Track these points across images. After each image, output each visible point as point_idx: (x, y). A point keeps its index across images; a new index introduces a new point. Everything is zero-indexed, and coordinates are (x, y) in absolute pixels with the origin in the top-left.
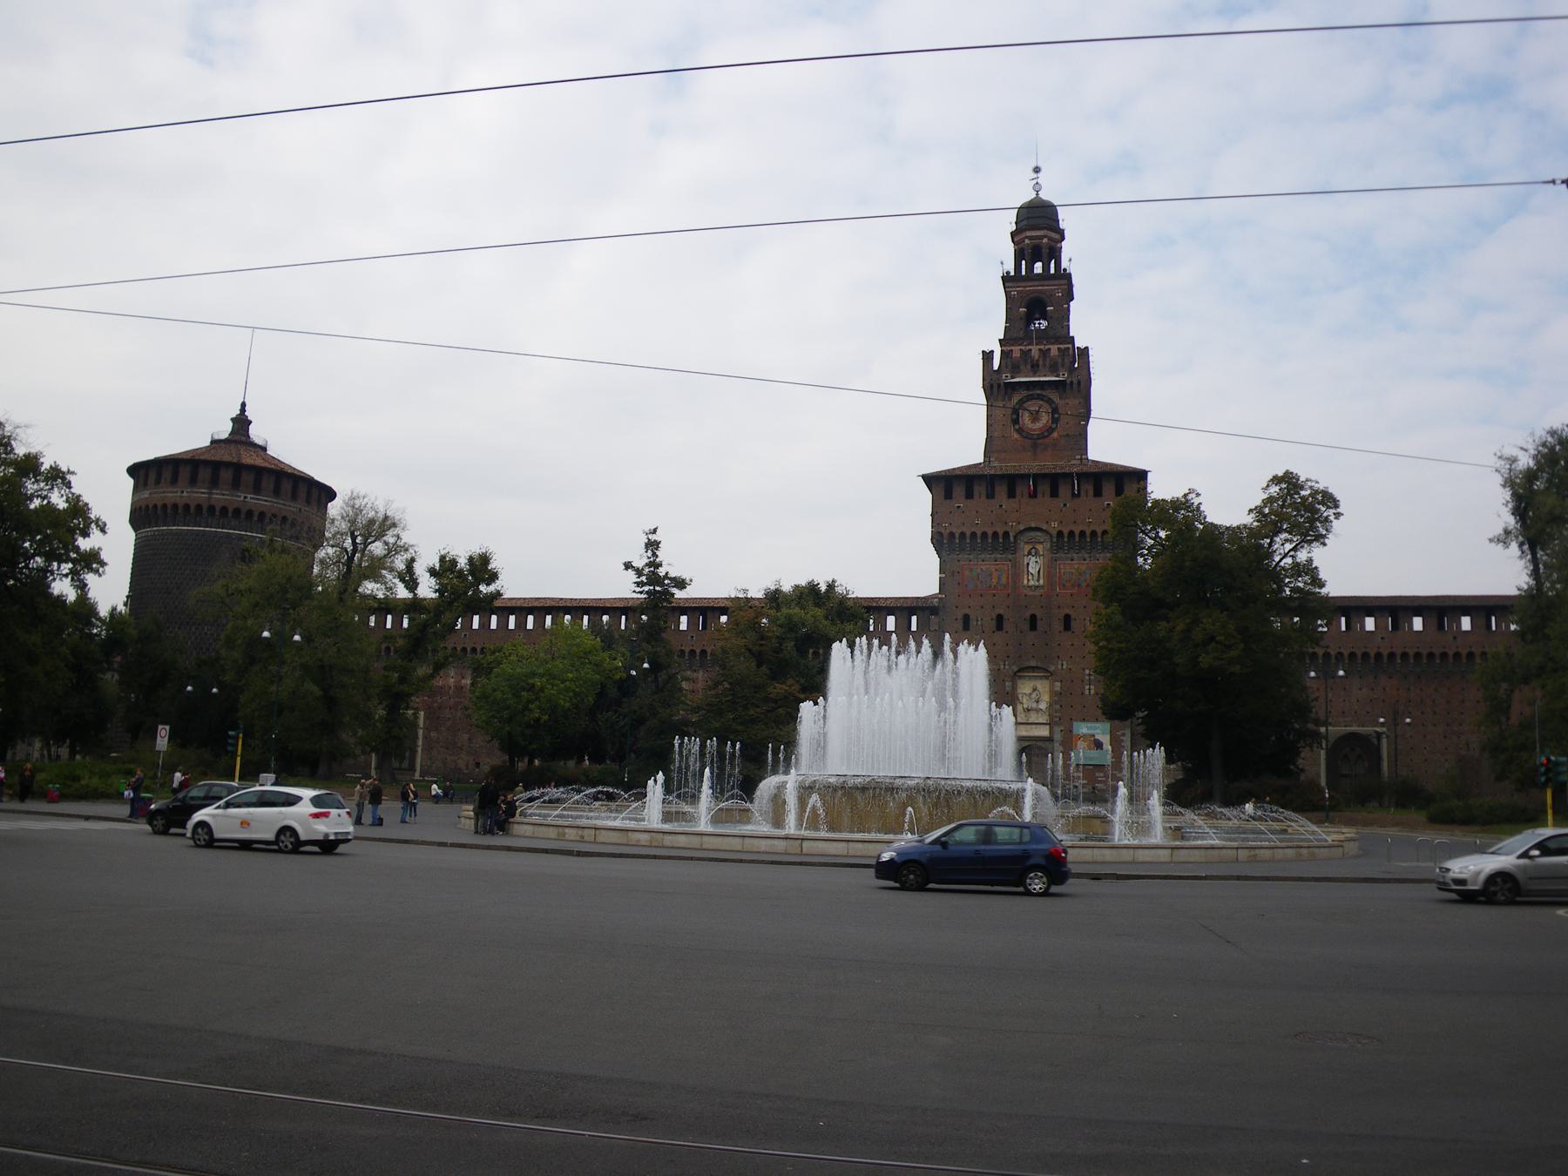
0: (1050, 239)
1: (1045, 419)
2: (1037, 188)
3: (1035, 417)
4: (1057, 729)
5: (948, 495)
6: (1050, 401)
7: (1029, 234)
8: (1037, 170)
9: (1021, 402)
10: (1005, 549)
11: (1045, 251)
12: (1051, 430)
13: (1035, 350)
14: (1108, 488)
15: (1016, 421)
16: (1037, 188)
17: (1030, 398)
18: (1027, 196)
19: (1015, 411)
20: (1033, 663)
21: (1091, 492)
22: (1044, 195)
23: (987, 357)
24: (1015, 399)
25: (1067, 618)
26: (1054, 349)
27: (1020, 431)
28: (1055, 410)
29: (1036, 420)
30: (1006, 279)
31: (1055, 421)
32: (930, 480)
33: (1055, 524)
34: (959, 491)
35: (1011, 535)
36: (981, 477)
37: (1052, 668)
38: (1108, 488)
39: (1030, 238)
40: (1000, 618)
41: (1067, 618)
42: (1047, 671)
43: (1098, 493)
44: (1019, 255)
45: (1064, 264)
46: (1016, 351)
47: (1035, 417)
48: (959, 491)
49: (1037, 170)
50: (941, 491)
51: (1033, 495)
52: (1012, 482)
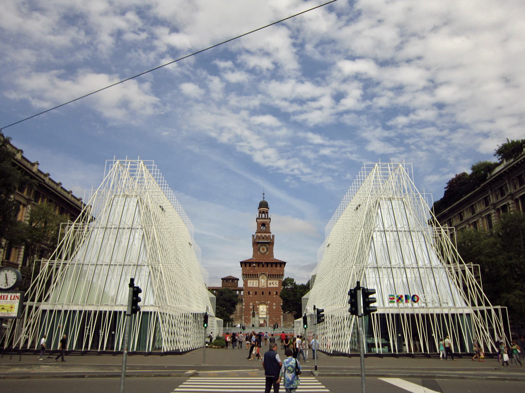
0: (266, 210)
1: (265, 250)
2: (264, 198)
3: (263, 249)
4: (268, 316)
5: (245, 266)
6: (266, 246)
7: (262, 209)
8: (264, 194)
9: (260, 246)
10: (258, 278)
11: (265, 213)
12: (266, 252)
13: (263, 235)
14: (278, 266)
15: (259, 250)
16: (264, 198)
17: (263, 245)
18: (262, 200)
19: (259, 248)
20: (263, 302)
21: (275, 266)
22: (265, 200)
23: (253, 236)
24: (259, 245)
25: (270, 293)
26: (267, 235)
27: (260, 252)
28: (267, 248)
29: (263, 249)
30: (257, 219)
31: (267, 250)
32: (241, 263)
33: (267, 273)
34: (248, 265)
35: (259, 275)
36: (253, 263)
37: (267, 303)
38: (278, 266)
39: (262, 210)
40: (256, 292)
41: (270, 293)
42: (265, 303)
43: (276, 266)
44: (260, 212)
45: (269, 216)
46: (259, 235)
47: (263, 249)
48: (248, 265)
49: (264, 194)
50: (243, 265)
51: (263, 266)
52: (258, 264)
